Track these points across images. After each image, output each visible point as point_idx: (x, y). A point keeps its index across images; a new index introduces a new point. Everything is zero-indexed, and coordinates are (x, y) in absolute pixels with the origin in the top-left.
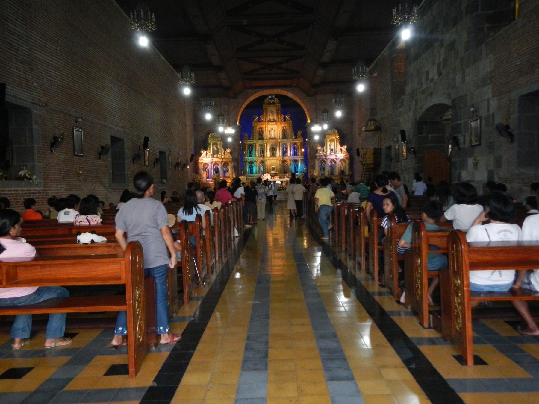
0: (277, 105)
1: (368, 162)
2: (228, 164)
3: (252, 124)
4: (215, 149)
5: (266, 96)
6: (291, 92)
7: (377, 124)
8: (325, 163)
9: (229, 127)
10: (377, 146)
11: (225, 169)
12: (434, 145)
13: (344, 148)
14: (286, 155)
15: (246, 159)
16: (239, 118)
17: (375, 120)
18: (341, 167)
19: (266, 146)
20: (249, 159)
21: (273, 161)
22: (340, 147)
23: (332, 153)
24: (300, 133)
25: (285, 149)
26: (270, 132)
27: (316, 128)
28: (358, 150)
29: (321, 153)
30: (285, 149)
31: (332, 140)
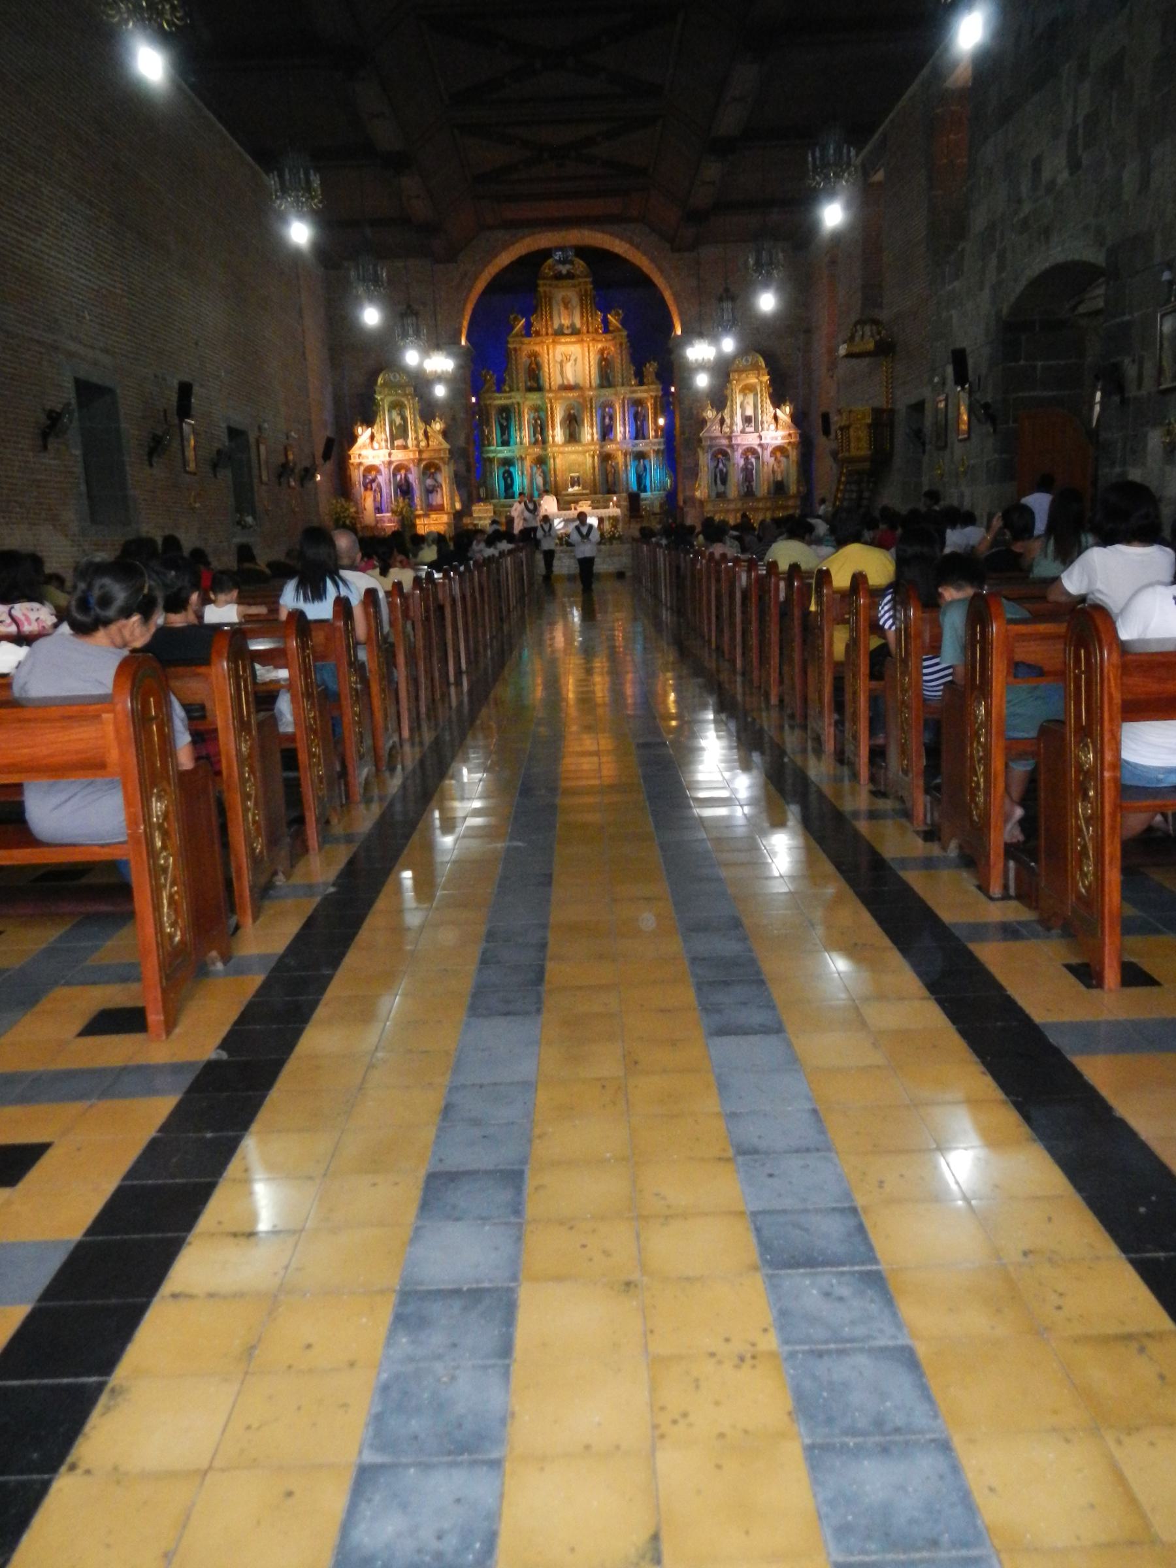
0: (581, 280)
1: (854, 452)
2: (438, 469)
3: (507, 342)
4: (398, 421)
5: (546, 254)
6: (622, 239)
7: (883, 332)
8: (729, 459)
9: (436, 353)
10: (881, 402)
11: (429, 482)
12: (1051, 394)
13: (785, 413)
14: (612, 437)
15: (493, 452)
16: (465, 323)
17: (875, 322)
18: (773, 472)
20: (500, 452)
21: (573, 457)
22: (771, 408)
23: (748, 429)
24: (651, 368)
25: (607, 420)
26: (562, 367)
27: (699, 352)
28: (826, 418)
29: (715, 430)
30: (607, 420)
31: (748, 389)
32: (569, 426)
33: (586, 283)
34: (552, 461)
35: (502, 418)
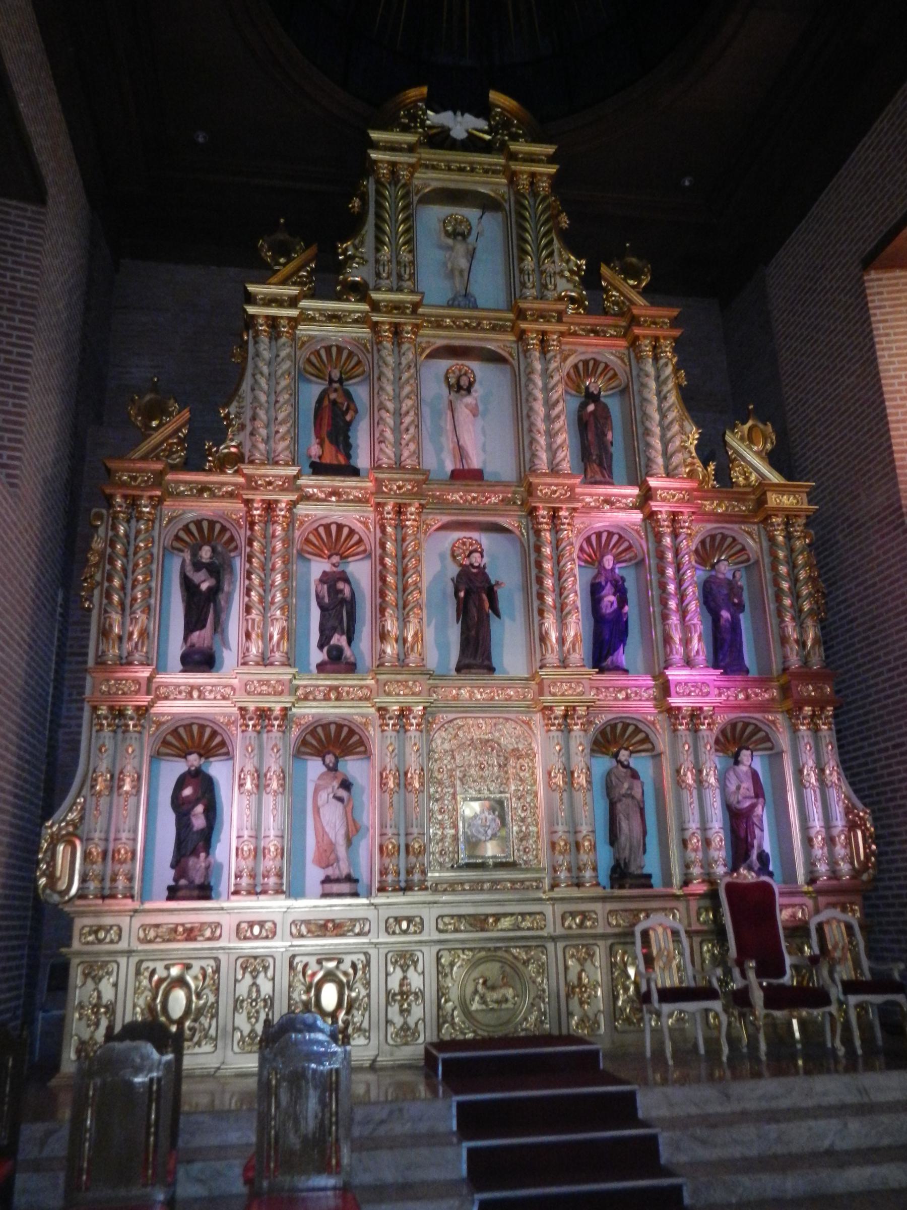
25: (609, 599)
30: (609, 599)
32: (463, 610)
33: (531, 159)
35: (198, 565)
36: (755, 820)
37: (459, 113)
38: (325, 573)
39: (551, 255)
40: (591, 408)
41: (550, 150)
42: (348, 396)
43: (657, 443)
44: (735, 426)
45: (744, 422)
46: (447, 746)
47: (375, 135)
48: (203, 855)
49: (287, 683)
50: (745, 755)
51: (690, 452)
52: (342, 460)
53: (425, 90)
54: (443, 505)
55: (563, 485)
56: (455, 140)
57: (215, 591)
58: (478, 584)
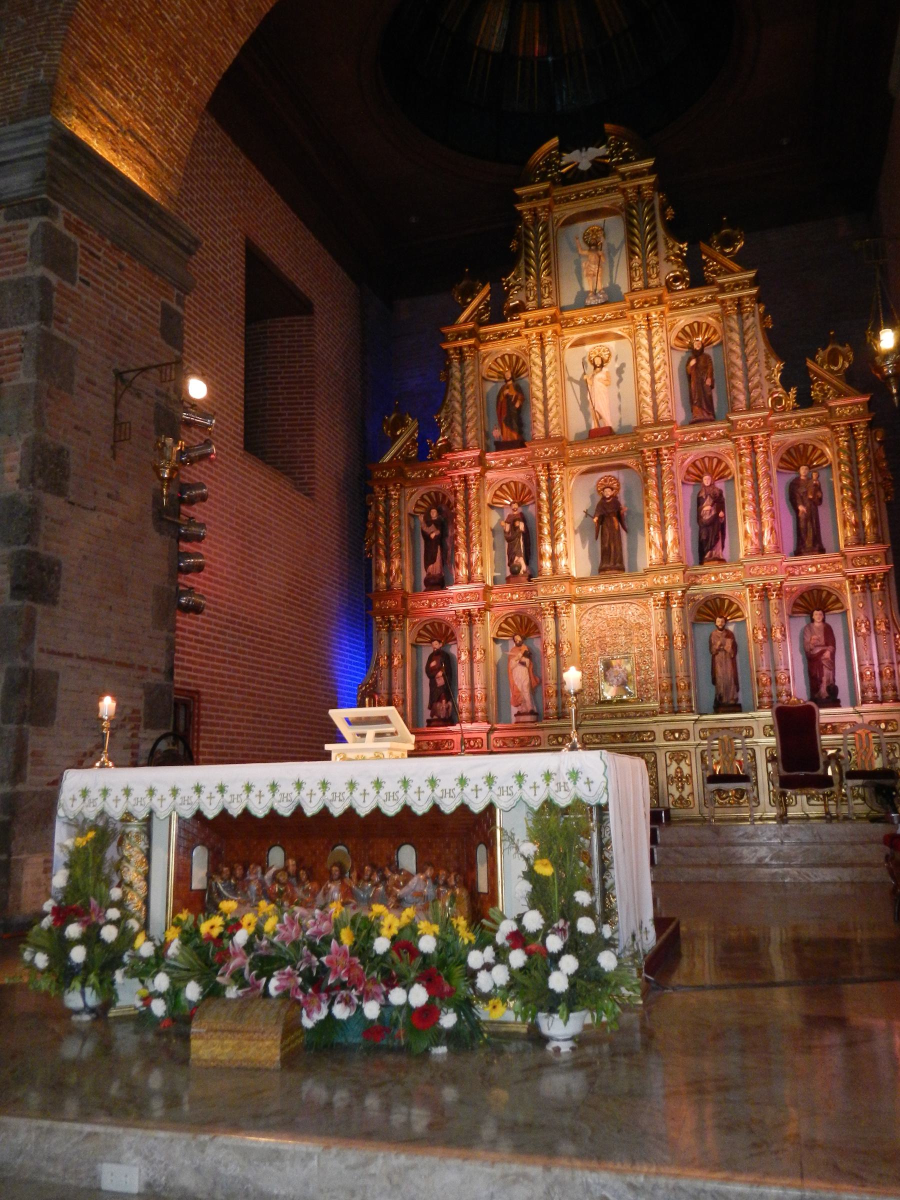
3: (444, 338)
19: (551, 499)
21: (611, 611)
25: (707, 508)
34: (550, 620)
36: (824, 662)
37: (584, 149)
38: (509, 516)
39: (654, 248)
40: (693, 362)
41: (650, 163)
42: (518, 389)
43: (740, 384)
44: (817, 352)
45: (824, 348)
46: (590, 625)
47: (518, 191)
48: (444, 701)
49: (481, 593)
50: (817, 615)
51: (775, 383)
52: (515, 436)
53: (555, 141)
54: (580, 459)
55: (663, 430)
56: (583, 172)
57: (441, 539)
58: (609, 511)
